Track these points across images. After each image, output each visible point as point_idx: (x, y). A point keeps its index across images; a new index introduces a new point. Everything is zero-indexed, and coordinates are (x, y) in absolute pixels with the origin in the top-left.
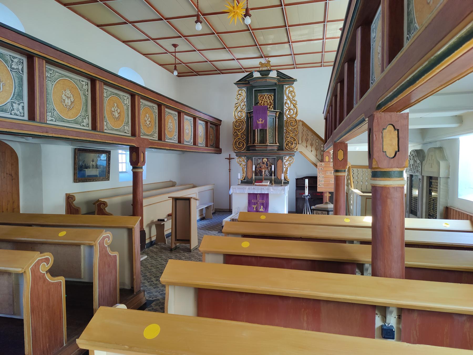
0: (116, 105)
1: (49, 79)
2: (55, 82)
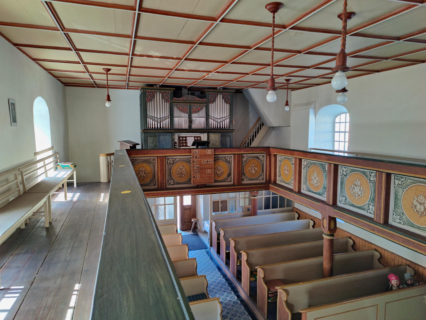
1: (400, 186)
2: (407, 189)
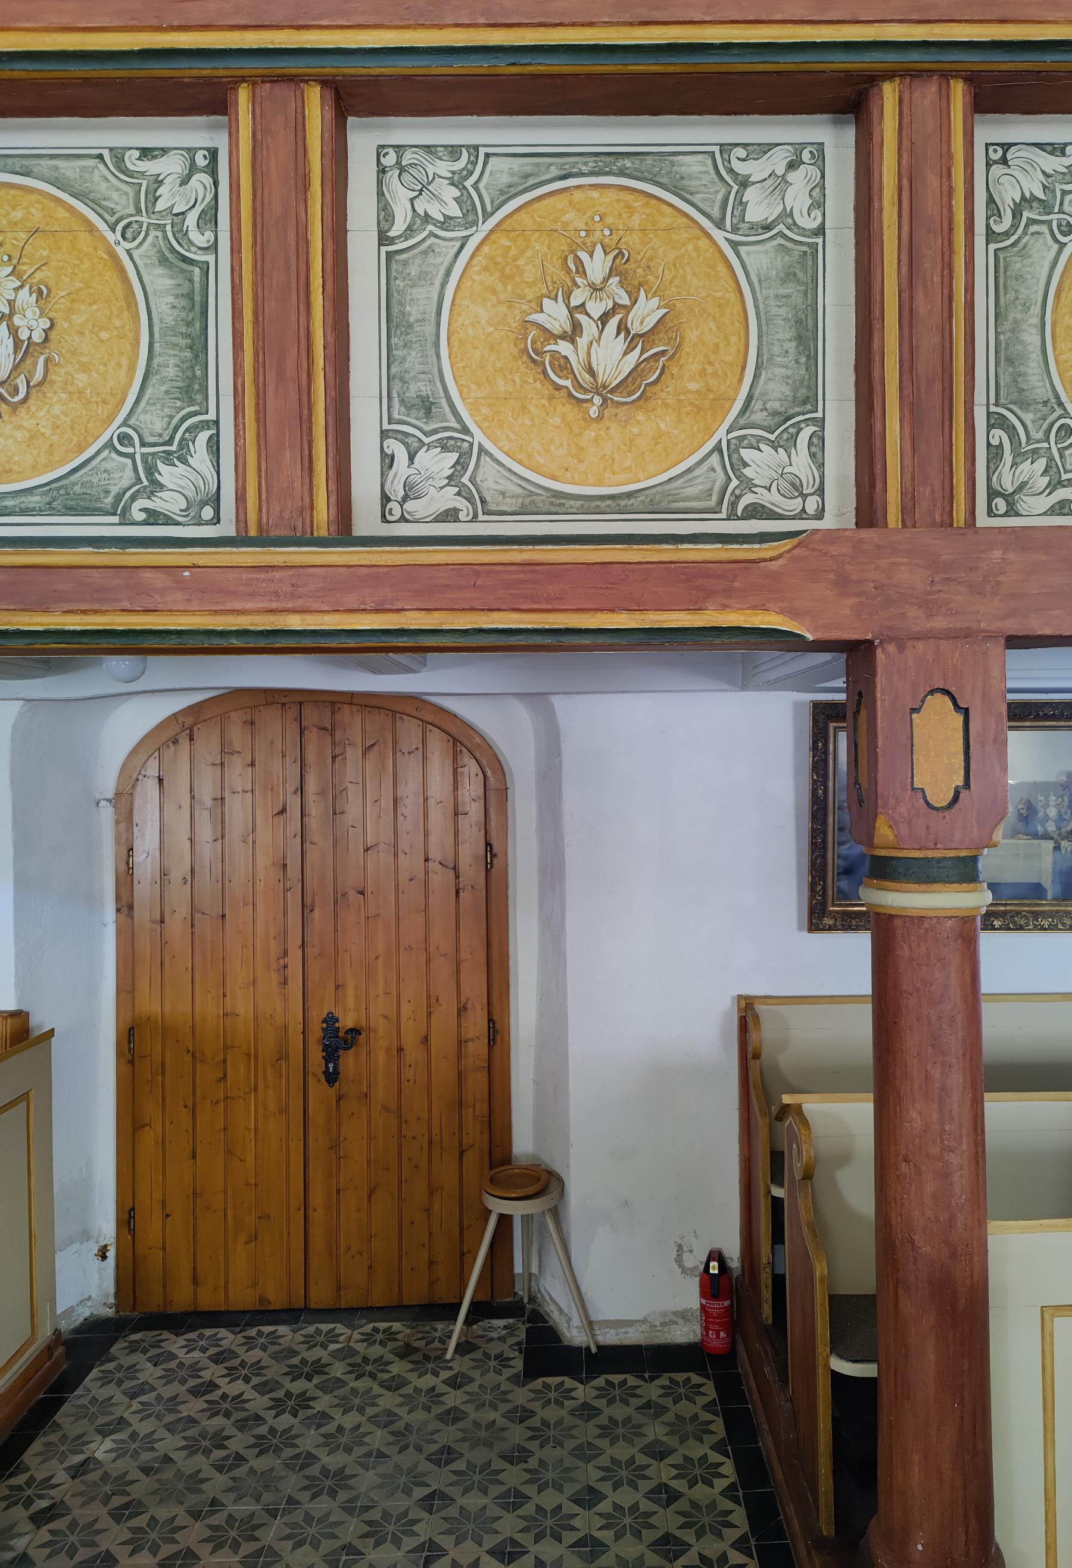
0: (597, 266)
